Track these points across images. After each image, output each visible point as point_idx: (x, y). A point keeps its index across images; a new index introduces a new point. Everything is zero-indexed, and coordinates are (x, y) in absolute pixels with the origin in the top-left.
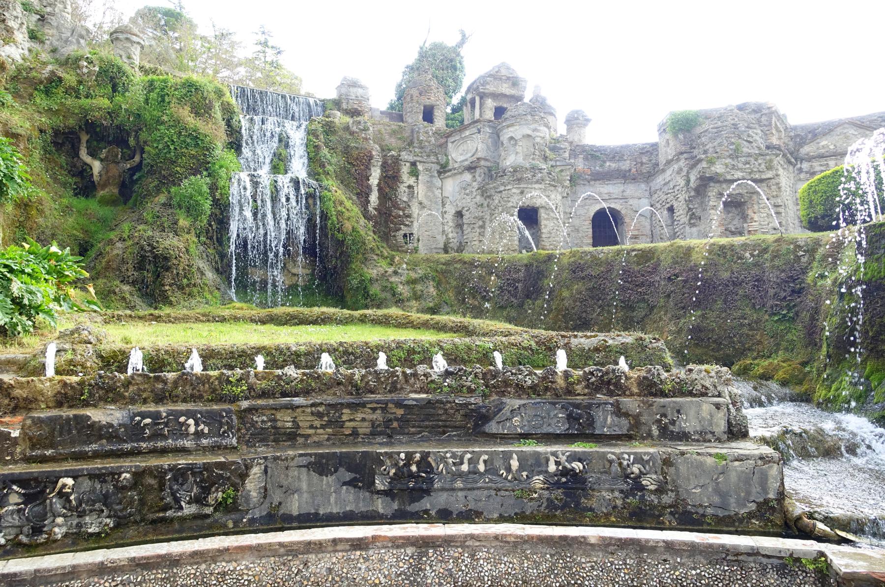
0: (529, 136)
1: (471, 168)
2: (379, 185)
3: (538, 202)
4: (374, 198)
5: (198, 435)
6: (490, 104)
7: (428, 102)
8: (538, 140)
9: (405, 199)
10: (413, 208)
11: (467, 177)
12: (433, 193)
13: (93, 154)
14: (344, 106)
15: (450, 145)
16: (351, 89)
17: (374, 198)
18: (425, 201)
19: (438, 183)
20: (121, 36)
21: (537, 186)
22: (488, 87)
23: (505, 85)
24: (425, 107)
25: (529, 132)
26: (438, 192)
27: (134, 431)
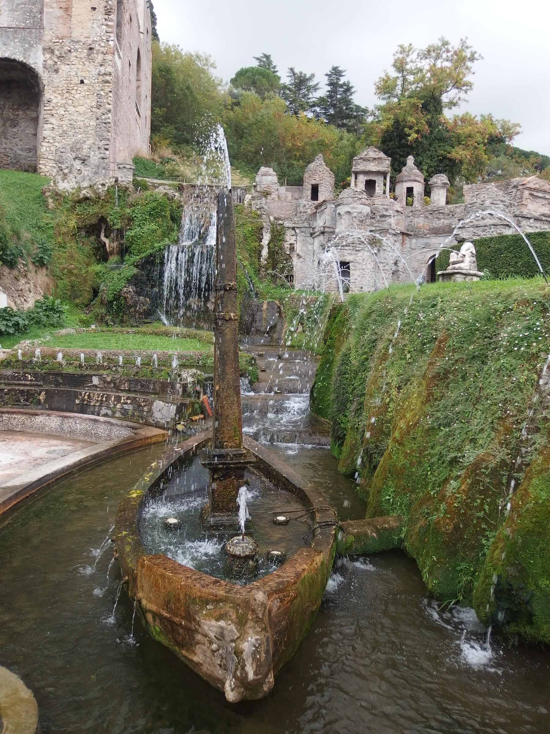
0: (349, 212)
1: (323, 233)
2: (269, 244)
3: (348, 258)
4: (265, 252)
5: (31, 380)
6: (362, 179)
7: (314, 182)
8: (355, 214)
9: (288, 253)
10: (294, 259)
11: (322, 237)
12: (307, 247)
13: (106, 237)
14: (258, 189)
15: (318, 215)
16: (264, 177)
17: (265, 252)
18: (301, 254)
19: (310, 240)
20: (121, 166)
21: (347, 248)
22: (358, 167)
23: (372, 164)
24: (312, 185)
25: (349, 210)
26: (310, 247)
27: (13, 377)
